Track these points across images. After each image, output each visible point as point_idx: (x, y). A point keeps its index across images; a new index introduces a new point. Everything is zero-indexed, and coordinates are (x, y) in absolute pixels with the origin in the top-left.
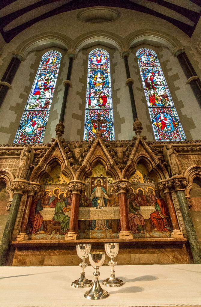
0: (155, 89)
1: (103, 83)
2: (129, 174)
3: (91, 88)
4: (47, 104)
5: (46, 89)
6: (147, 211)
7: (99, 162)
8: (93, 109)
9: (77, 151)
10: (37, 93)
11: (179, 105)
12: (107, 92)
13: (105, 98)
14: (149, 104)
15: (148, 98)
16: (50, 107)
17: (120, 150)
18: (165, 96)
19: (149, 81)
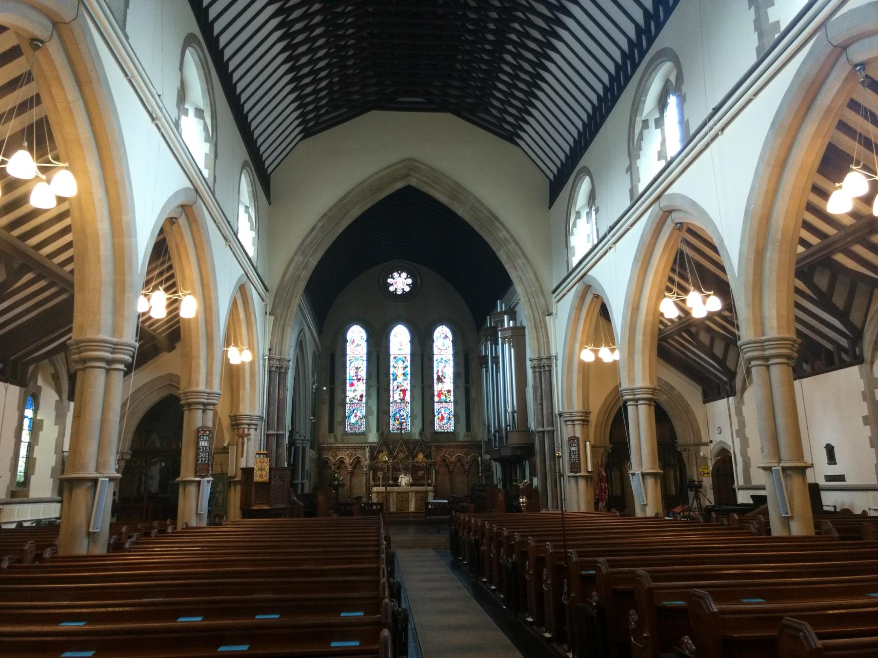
0: (442, 382)
1: (404, 374)
2: (416, 456)
3: (394, 380)
4: (362, 396)
5: (359, 380)
6: (421, 473)
7: (401, 451)
8: (395, 402)
9: (391, 446)
10: (352, 385)
11: (455, 402)
12: (407, 385)
13: (404, 391)
14: (436, 399)
15: (436, 393)
16: (364, 399)
17: (411, 446)
18: (449, 391)
19: (440, 374)
